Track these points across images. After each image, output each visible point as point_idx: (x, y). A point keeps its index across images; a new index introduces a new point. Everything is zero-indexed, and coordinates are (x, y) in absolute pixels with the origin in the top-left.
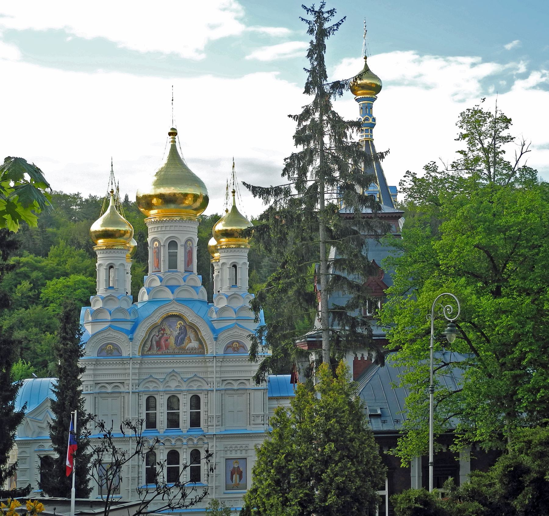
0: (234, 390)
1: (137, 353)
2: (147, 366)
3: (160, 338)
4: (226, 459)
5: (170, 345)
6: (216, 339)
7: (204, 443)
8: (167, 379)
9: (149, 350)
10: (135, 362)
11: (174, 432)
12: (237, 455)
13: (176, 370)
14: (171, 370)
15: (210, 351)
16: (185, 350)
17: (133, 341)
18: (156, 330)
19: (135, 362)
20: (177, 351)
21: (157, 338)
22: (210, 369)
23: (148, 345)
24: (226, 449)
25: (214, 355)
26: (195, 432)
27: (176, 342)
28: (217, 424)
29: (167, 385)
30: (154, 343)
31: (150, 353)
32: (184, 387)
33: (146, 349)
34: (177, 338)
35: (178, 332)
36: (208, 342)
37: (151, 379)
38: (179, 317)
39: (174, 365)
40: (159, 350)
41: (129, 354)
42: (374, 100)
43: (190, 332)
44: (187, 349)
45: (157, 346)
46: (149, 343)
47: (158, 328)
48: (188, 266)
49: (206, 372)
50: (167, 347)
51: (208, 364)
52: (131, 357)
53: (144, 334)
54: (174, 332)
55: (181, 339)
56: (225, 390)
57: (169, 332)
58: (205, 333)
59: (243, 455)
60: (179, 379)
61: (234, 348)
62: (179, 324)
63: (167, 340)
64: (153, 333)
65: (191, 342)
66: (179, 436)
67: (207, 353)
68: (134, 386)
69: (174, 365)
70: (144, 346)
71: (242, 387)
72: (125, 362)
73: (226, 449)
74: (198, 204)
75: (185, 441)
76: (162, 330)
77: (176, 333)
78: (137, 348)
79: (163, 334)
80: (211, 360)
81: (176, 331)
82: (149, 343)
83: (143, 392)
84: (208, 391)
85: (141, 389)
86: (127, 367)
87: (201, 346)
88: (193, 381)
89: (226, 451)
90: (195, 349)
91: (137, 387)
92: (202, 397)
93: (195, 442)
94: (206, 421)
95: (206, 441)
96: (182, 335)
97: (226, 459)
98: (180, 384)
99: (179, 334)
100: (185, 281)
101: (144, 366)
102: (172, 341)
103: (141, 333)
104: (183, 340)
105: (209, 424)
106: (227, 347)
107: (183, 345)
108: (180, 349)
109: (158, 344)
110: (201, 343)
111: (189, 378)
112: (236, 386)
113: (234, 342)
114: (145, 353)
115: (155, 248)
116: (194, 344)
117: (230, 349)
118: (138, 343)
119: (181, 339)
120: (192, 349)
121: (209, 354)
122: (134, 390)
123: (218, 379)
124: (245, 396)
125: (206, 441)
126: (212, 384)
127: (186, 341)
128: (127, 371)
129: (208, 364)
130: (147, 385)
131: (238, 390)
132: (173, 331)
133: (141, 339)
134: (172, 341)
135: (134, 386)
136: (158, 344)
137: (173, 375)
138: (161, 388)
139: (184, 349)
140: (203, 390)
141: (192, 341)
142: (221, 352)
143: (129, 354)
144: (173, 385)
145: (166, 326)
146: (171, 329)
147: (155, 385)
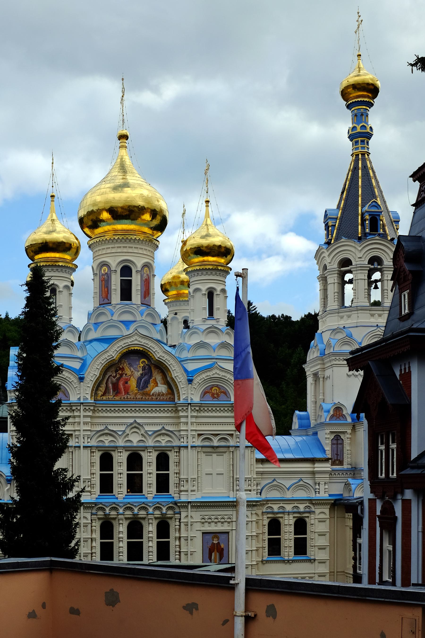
0: (213, 447)
1: (89, 396)
2: (101, 414)
3: (118, 380)
4: (203, 533)
5: (131, 388)
6: (190, 381)
7: (175, 513)
8: (127, 432)
9: (103, 395)
10: (87, 408)
11: (135, 499)
12: (210, 528)
13: (139, 421)
14: (132, 421)
15: (182, 397)
16: (149, 395)
17: (84, 381)
18: (113, 369)
19: (87, 408)
20: (139, 396)
21: (114, 380)
22: (183, 420)
23: (103, 388)
24: (203, 521)
25: (189, 402)
26: (163, 498)
27: (138, 386)
28: (193, 489)
29: (127, 439)
30: (110, 385)
31: (104, 398)
32: (150, 442)
33: (100, 393)
34: (139, 380)
35: (141, 372)
36: (180, 386)
37: (107, 431)
38: (142, 354)
39: (137, 414)
40: (116, 395)
41: (79, 399)
42: (371, 105)
43: (156, 373)
44: (153, 395)
45: (114, 390)
46: (104, 385)
47: (113, 367)
48: (145, 297)
49: (178, 424)
50: (127, 392)
51: (181, 414)
52: (82, 401)
53: (98, 373)
54: (136, 373)
55: (144, 383)
56: (202, 447)
57: (129, 373)
58: (177, 373)
59: (225, 527)
60: (143, 432)
61: (213, 395)
62: (142, 363)
63: (126, 383)
64: (109, 374)
65: (157, 386)
66: (144, 503)
67: (179, 399)
68: (86, 438)
69: (137, 414)
70: (97, 389)
71: (223, 444)
72: (74, 408)
73: (203, 521)
74: (156, 222)
75: (151, 510)
76: (120, 369)
77: (138, 374)
78: (89, 391)
79: (121, 375)
80: (185, 408)
81: (138, 371)
82: (104, 385)
83: (97, 447)
84: (180, 447)
85: (93, 443)
86: (76, 414)
87: (170, 391)
88: (160, 435)
89: (203, 523)
90: (163, 395)
91: (89, 440)
92: (172, 456)
93: (164, 511)
94: (178, 485)
95: (177, 510)
96: (146, 377)
97: (203, 533)
98: (143, 439)
99: (142, 374)
100: (142, 315)
101: (97, 415)
102: (133, 383)
103: (93, 373)
104: (147, 383)
105: (182, 488)
106: (204, 393)
107: (147, 389)
108: (144, 394)
109: (116, 387)
110: (170, 387)
111: (155, 432)
112: (216, 443)
113: (213, 386)
114: (99, 398)
115: (103, 275)
116: (162, 388)
117: (208, 396)
118: (91, 385)
119: (144, 383)
120: (159, 395)
121: (182, 401)
122: (86, 444)
123: (194, 433)
124: (226, 455)
125: (177, 510)
126: (185, 438)
128: (77, 420)
129: (181, 414)
130: (102, 438)
131: (218, 447)
132: (134, 372)
133: (94, 379)
134: (133, 383)
135: (86, 438)
136: (116, 387)
137: (135, 427)
138: (121, 443)
139: (148, 394)
140: (173, 447)
141: (159, 385)
142: (197, 399)
143: (79, 399)
144: (135, 439)
145: (126, 366)
146: (132, 369)
147: (111, 438)
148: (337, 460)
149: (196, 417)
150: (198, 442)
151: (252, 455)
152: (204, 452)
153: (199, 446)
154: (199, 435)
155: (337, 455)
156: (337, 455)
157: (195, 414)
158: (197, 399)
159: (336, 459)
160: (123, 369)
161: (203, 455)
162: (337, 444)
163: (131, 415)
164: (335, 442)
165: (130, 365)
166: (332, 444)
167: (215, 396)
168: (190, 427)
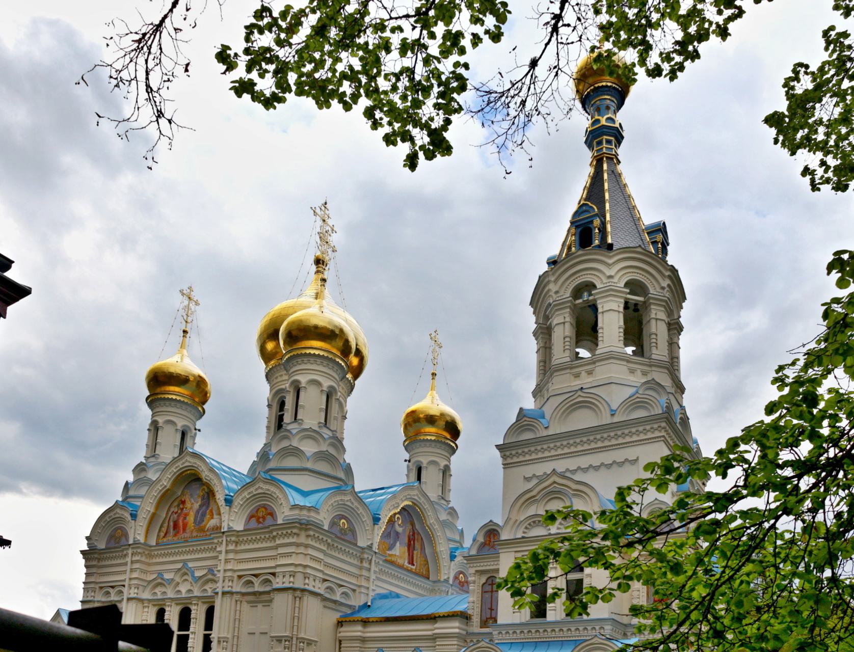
20: (195, 534)
30: (172, 524)
31: (165, 540)
33: (162, 534)
34: (198, 512)
63: (185, 518)
64: (172, 510)
79: (182, 509)
82: (166, 525)
99: (200, 506)
109: (176, 526)
112: (257, 588)
117: (254, 520)
127: (208, 516)
134: (191, 518)
138: (171, 594)
148: (491, 618)
149: (236, 552)
150: (238, 587)
151: (297, 602)
152: (248, 602)
153: (237, 593)
154: (240, 577)
155: (491, 609)
156: (491, 609)
157: (231, 547)
158: (239, 526)
159: (489, 616)
160: (183, 502)
161: (245, 605)
162: (492, 591)
163: (178, 558)
164: (488, 588)
165: (191, 496)
166: (484, 592)
167: (261, 520)
168: (229, 564)
